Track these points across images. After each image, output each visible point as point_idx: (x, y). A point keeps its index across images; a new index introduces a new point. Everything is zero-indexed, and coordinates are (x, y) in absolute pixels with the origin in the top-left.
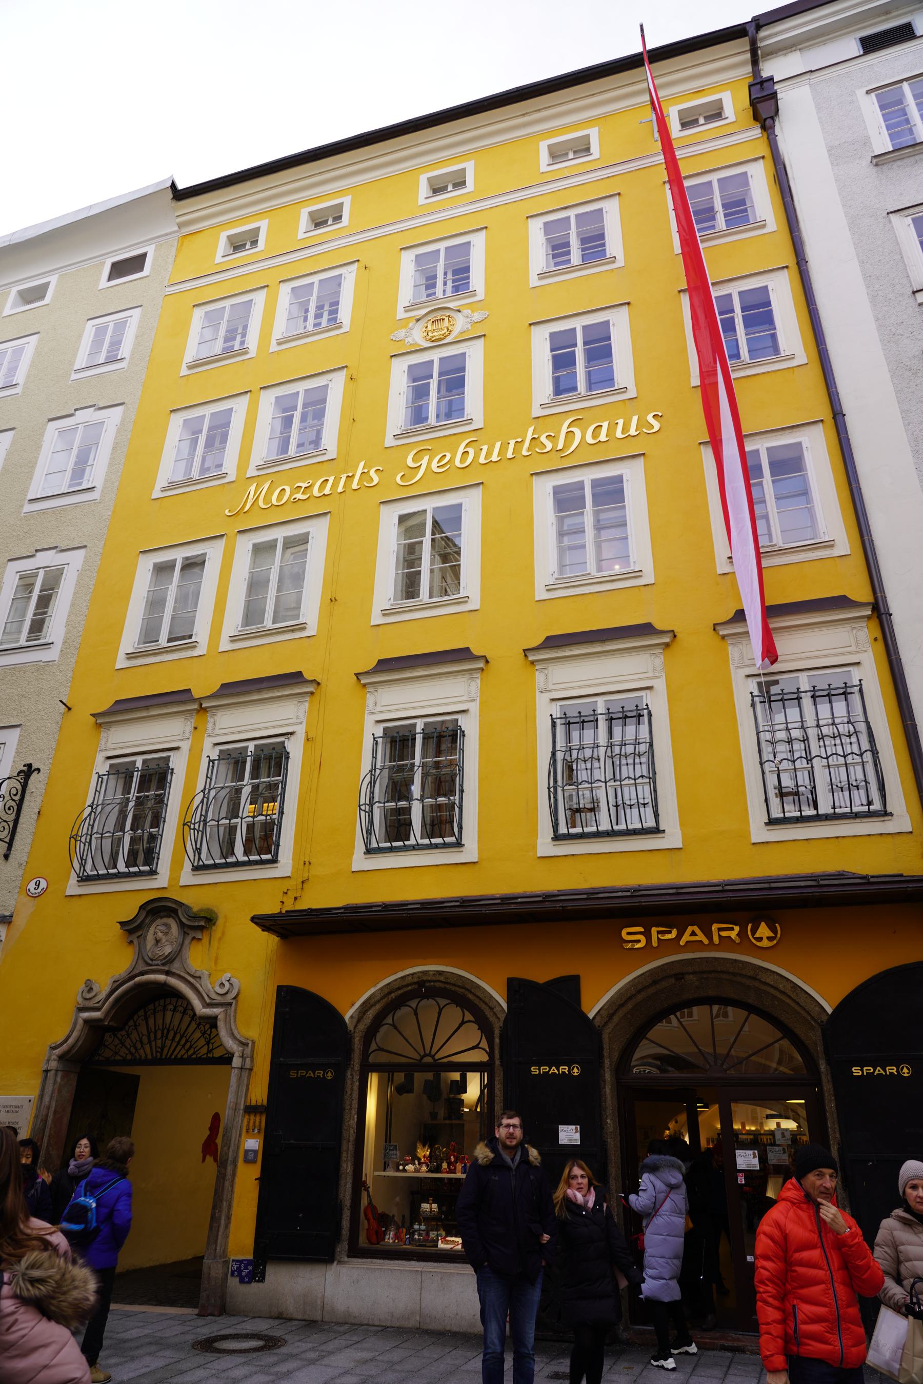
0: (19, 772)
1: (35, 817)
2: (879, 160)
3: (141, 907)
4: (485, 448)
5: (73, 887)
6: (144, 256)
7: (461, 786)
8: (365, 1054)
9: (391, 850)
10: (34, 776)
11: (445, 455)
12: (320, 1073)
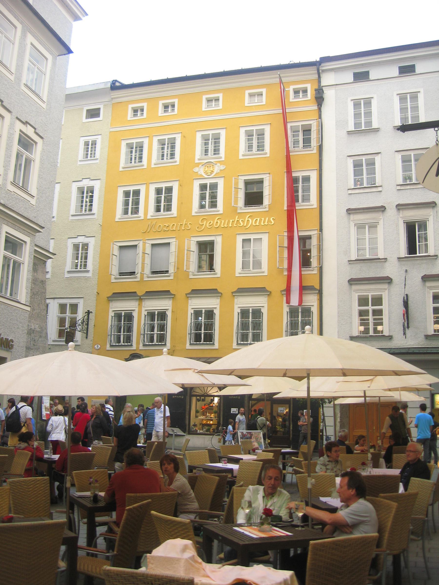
0: (86, 312)
1: (93, 326)
2: (349, 133)
3: (130, 355)
4: (223, 221)
5: (108, 347)
6: (99, 109)
7: (214, 329)
8: (191, 393)
9: (196, 344)
10: (91, 314)
11: (211, 222)
12: (180, 397)
